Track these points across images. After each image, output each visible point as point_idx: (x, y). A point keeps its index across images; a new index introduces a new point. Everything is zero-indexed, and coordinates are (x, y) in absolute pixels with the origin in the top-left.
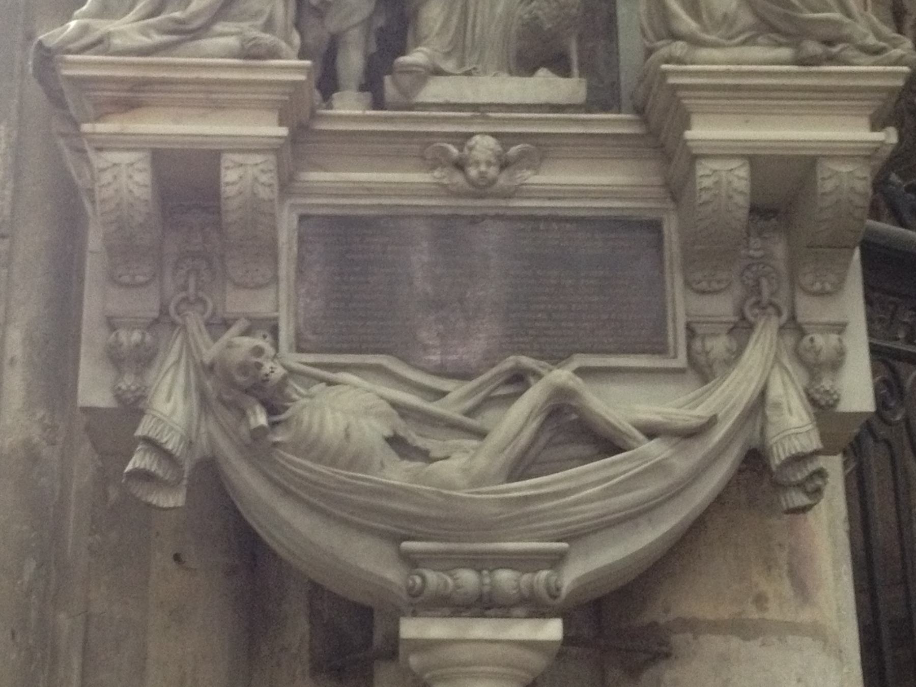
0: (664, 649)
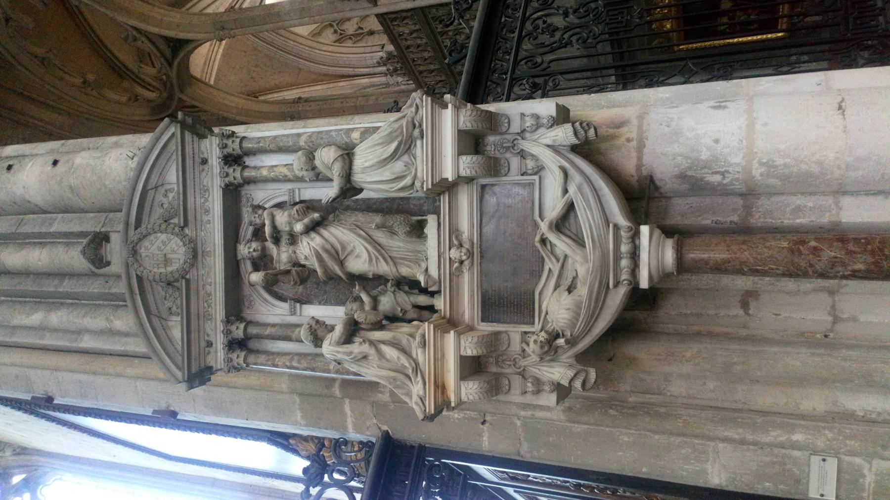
0: (649, 178)
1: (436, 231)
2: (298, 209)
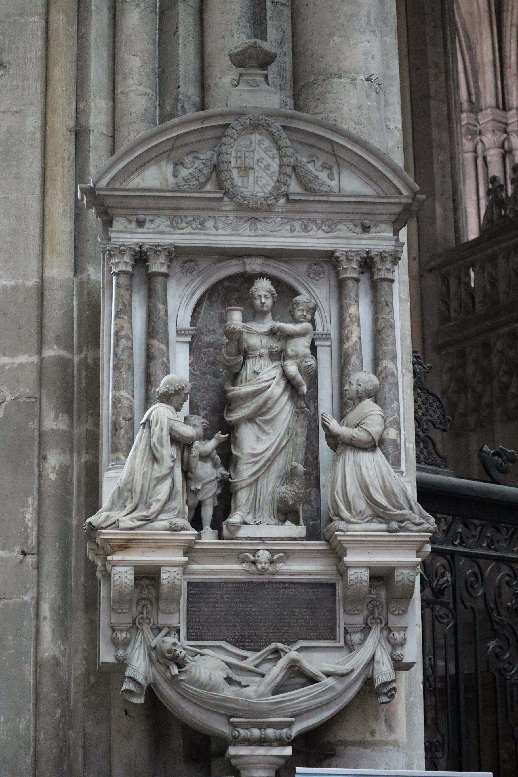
0: (333, 753)
1: (288, 536)
2: (312, 366)
